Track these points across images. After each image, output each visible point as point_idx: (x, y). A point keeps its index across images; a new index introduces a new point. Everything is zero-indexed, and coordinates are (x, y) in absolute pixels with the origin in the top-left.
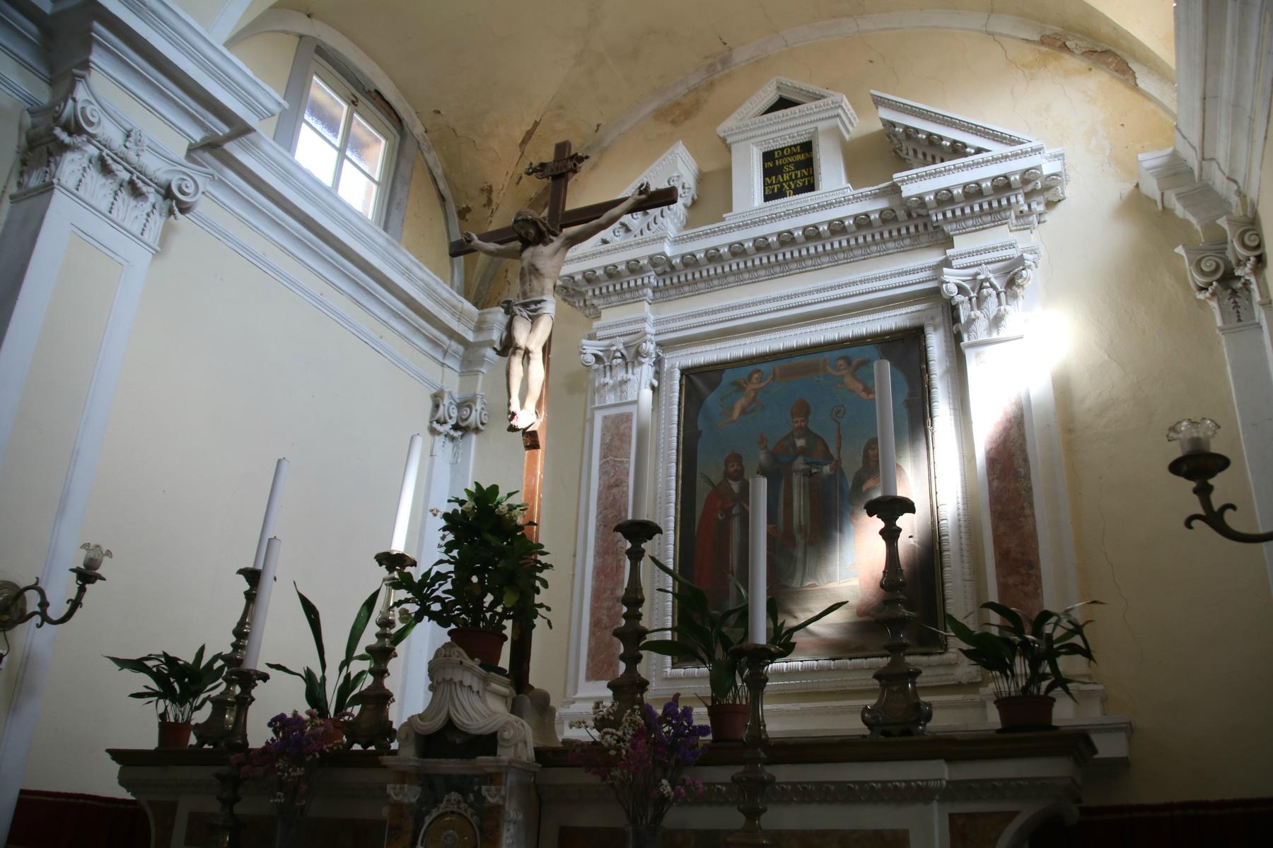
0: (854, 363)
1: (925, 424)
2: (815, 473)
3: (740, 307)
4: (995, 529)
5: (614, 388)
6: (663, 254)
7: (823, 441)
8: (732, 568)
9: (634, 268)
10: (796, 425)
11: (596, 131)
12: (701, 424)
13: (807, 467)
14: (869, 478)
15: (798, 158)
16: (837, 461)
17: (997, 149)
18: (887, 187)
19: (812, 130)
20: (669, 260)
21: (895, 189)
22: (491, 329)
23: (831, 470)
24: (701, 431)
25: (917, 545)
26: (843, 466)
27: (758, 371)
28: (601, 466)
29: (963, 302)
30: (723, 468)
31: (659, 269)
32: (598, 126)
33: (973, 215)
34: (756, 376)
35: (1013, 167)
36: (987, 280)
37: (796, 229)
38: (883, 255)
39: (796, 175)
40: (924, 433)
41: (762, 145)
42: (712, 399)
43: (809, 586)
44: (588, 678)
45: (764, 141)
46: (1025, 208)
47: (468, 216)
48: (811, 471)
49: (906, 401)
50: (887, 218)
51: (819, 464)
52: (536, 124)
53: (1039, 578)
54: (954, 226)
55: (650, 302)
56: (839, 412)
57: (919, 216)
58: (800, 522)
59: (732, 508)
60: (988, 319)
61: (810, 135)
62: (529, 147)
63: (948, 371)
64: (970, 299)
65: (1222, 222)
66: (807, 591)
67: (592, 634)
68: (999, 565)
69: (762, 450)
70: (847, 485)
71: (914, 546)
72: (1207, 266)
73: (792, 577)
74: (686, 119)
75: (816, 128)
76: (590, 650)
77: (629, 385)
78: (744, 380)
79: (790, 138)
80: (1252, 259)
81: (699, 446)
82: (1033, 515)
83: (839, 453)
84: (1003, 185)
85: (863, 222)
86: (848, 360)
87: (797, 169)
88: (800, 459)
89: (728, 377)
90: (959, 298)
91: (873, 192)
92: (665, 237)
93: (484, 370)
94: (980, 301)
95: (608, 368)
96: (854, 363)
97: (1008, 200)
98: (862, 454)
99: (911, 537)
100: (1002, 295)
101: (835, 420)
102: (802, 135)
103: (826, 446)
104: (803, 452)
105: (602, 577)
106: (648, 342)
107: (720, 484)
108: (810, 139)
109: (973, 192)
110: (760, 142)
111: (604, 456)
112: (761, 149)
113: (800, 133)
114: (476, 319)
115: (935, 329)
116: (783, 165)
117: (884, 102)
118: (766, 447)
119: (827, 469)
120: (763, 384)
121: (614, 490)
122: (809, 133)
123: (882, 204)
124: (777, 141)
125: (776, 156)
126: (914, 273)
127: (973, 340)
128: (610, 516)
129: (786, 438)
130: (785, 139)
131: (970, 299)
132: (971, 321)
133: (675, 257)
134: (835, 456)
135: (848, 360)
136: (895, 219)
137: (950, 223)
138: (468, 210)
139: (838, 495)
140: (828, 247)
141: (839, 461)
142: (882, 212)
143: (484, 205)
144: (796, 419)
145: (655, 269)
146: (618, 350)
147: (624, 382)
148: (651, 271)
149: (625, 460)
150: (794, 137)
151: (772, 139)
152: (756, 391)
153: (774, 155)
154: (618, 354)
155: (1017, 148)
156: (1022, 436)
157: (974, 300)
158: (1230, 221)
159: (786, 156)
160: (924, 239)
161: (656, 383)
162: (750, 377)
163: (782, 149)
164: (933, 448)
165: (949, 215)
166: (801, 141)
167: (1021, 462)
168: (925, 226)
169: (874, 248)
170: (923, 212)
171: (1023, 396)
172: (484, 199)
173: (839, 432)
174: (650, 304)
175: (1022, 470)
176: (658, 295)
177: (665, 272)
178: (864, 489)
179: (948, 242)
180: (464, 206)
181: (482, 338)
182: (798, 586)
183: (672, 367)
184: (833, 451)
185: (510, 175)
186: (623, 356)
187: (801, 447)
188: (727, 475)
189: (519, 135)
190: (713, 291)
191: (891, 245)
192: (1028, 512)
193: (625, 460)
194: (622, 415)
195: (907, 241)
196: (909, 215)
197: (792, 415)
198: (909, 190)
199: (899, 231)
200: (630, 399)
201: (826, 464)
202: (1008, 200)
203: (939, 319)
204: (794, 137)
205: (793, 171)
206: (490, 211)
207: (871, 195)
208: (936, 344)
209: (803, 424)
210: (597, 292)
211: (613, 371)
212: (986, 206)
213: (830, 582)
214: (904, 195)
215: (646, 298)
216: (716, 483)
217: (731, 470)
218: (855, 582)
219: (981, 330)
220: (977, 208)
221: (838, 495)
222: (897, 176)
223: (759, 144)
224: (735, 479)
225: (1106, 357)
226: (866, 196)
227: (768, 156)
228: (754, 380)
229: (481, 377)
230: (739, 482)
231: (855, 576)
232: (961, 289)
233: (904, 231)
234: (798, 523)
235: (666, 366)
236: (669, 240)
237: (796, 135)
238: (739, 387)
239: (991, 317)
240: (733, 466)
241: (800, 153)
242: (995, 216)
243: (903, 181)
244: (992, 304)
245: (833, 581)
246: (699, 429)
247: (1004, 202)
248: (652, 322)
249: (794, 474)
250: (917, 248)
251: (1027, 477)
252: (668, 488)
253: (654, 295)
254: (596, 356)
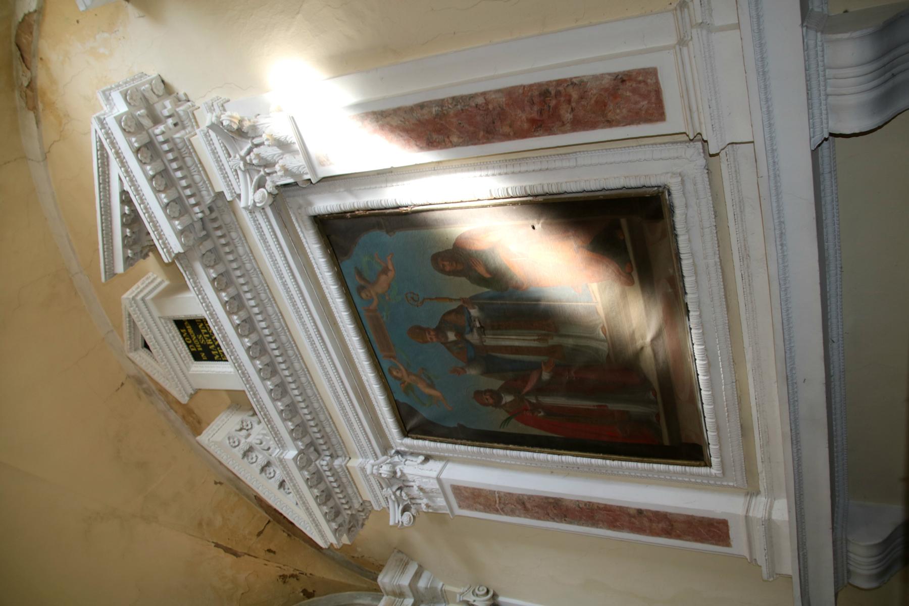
0: (362, 283)
1: (407, 214)
2: (480, 323)
4: (507, 137)
5: (430, 498)
7: (444, 315)
8: (594, 406)
9: (317, 478)
10: (435, 340)
11: (221, 483)
12: (453, 424)
13: (475, 330)
14: (476, 271)
15: (191, 331)
16: (464, 302)
18: (181, 264)
19: (163, 321)
20: (301, 452)
22: (399, 586)
23: (474, 308)
24: (458, 424)
25: (542, 221)
26: (468, 297)
27: (390, 371)
28: (506, 514)
29: (273, 182)
30: (490, 408)
32: (216, 483)
34: (395, 373)
36: (243, 159)
38: (253, 256)
39: (205, 333)
40: (417, 214)
41: (188, 363)
42: (425, 413)
43: (605, 335)
44: (728, 545)
45: (183, 361)
46: (170, 121)
47: (311, 590)
48: (479, 327)
49: (387, 232)
50: (213, 258)
51: (470, 319)
52: (217, 545)
53: (559, 82)
54: (204, 193)
55: (348, 458)
56: (412, 298)
57: (204, 228)
58: (534, 340)
59: (530, 402)
60: (283, 154)
61: (168, 322)
62: (239, 550)
63: (350, 191)
64: (269, 174)
66: (610, 336)
67: (679, 537)
68: (549, 131)
69: (466, 372)
70: (488, 292)
71: (542, 224)
73: (597, 350)
74: (194, 413)
75: (159, 317)
76: (696, 541)
77: (424, 486)
78: (401, 384)
79: (175, 340)
81: (473, 427)
82: (484, 94)
83: (455, 300)
86: (360, 289)
87: (201, 333)
88: (469, 337)
89: (402, 398)
90: (269, 186)
91: (189, 277)
92: (279, 458)
93: (440, 585)
94: (268, 164)
95: (413, 501)
96: (362, 283)
98: (452, 277)
99: (534, 228)
100: (256, 141)
101: (422, 303)
102: (170, 329)
103: (450, 313)
104: (460, 334)
105: (618, 524)
106: (380, 472)
107: (507, 411)
108: (172, 321)
110: (185, 364)
111: (497, 511)
112: (192, 363)
113: (168, 331)
114: (393, 598)
115: (310, 204)
116: (200, 344)
117: (110, 269)
118: (462, 368)
119: (474, 312)
120: (402, 367)
121: (528, 506)
122: (166, 323)
124: (181, 351)
125: (195, 349)
126: (261, 228)
127: (306, 170)
128: (555, 511)
129: (449, 348)
130: (177, 344)
131: (269, 174)
132: (287, 172)
133: (297, 447)
134: (459, 303)
135: (360, 289)
138: (305, 591)
139: (499, 302)
141: (463, 300)
142: (206, 267)
143: (297, 579)
144: (429, 340)
145: (314, 460)
146: (394, 493)
148: (316, 465)
149: (497, 495)
150: (173, 336)
151: (180, 355)
152: (409, 374)
153: (194, 351)
155: (106, 144)
156: (396, 111)
157: (267, 171)
159: (192, 341)
162: (396, 378)
163: (188, 345)
164: (430, 204)
166: (176, 328)
167: (425, 111)
170: (198, 226)
171: (352, 113)
172: (292, 581)
173: (433, 299)
174: (350, 458)
175: (435, 110)
176: (340, 453)
177: (316, 450)
178: (487, 276)
180: (302, 594)
181: (407, 591)
182: (606, 344)
184: (454, 306)
185: (266, 562)
186: (400, 489)
187: (456, 336)
188: (497, 403)
189: (230, 558)
190: (325, 406)
191: (241, 250)
192: (480, 101)
193: (497, 495)
194: (454, 493)
197: (426, 342)
200: (437, 486)
201: (469, 313)
203: (300, 201)
204: (173, 336)
205: (202, 335)
206: (302, 575)
207: (193, 278)
208: (326, 204)
209: (432, 333)
211: (415, 497)
213: (597, 312)
215: (343, 464)
216: (507, 415)
217: (491, 401)
218: (594, 287)
219: (295, 162)
221: (499, 302)
223: (187, 365)
224: (501, 399)
225: (299, 16)
226: (195, 282)
227: (197, 357)
228: (399, 375)
229: (448, 588)
230: (503, 395)
231: (587, 286)
232: (260, 185)
234: (536, 342)
236: (282, 453)
237: (171, 335)
238: (409, 389)
239: (279, 151)
240: (487, 399)
241: (187, 329)
243: (169, 252)
244: (268, 152)
245: (596, 309)
246: (456, 426)
247: (166, 147)
248: (364, 460)
249: (485, 344)
250: (239, 224)
251: (441, 103)
252: (519, 458)
253: (341, 456)
254: (404, 511)
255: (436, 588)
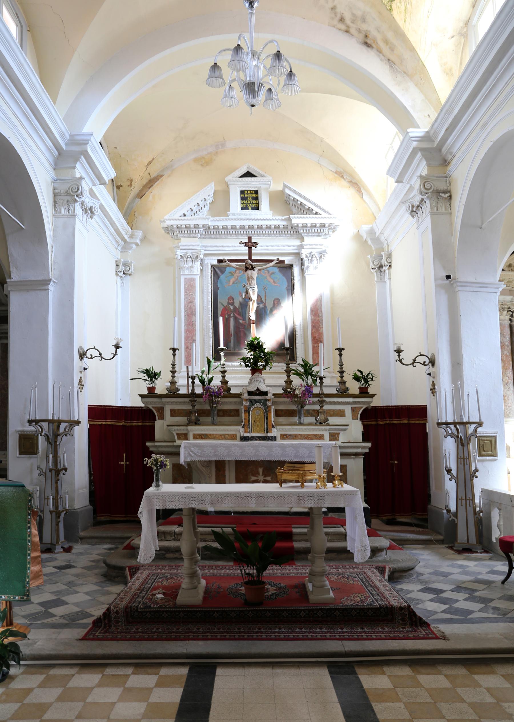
3: (232, 246)
6: (208, 225)
9: (196, 227)
17: (324, 214)
21: (290, 220)
31: (205, 228)
33: (312, 232)
35: (327, 222)
37: (255, 225)
54: (305, 234)
65: (383, 253)
72: (376, 263)
80: (388, 266)
84: (323, 226)
85: (277, 227)
97: (323, 230)
109: (314, 226)
123: (285, 223)
133: (212, 226)
136: (287, 228)
137: (304, 233)
140: (264, 232)
147: (192, 267)
154: (189, 257)
158: (385, 254)
160: (295, 236)
161: (202, 268)
165: (305, 231)
168: (296, 232)
169: (279, 235)
170: (297, 228)
177: (206, 229)
179: (302, 239)
183: (208, 263)
191: (284, 235)
195: (290, 235)
196: (292, 227)
198: (295, 221)
199: (288, 232)
202: (323, 230)
210: (180, 232)
212: (316, 231)
214: (293, 223)
220: (313, 231)
222: (291, 216)
233: (289, 232)
235: (205, 262)
242: (318, 233)
247: (322, 231)
254: (181, 256)
255: (130, 250)
